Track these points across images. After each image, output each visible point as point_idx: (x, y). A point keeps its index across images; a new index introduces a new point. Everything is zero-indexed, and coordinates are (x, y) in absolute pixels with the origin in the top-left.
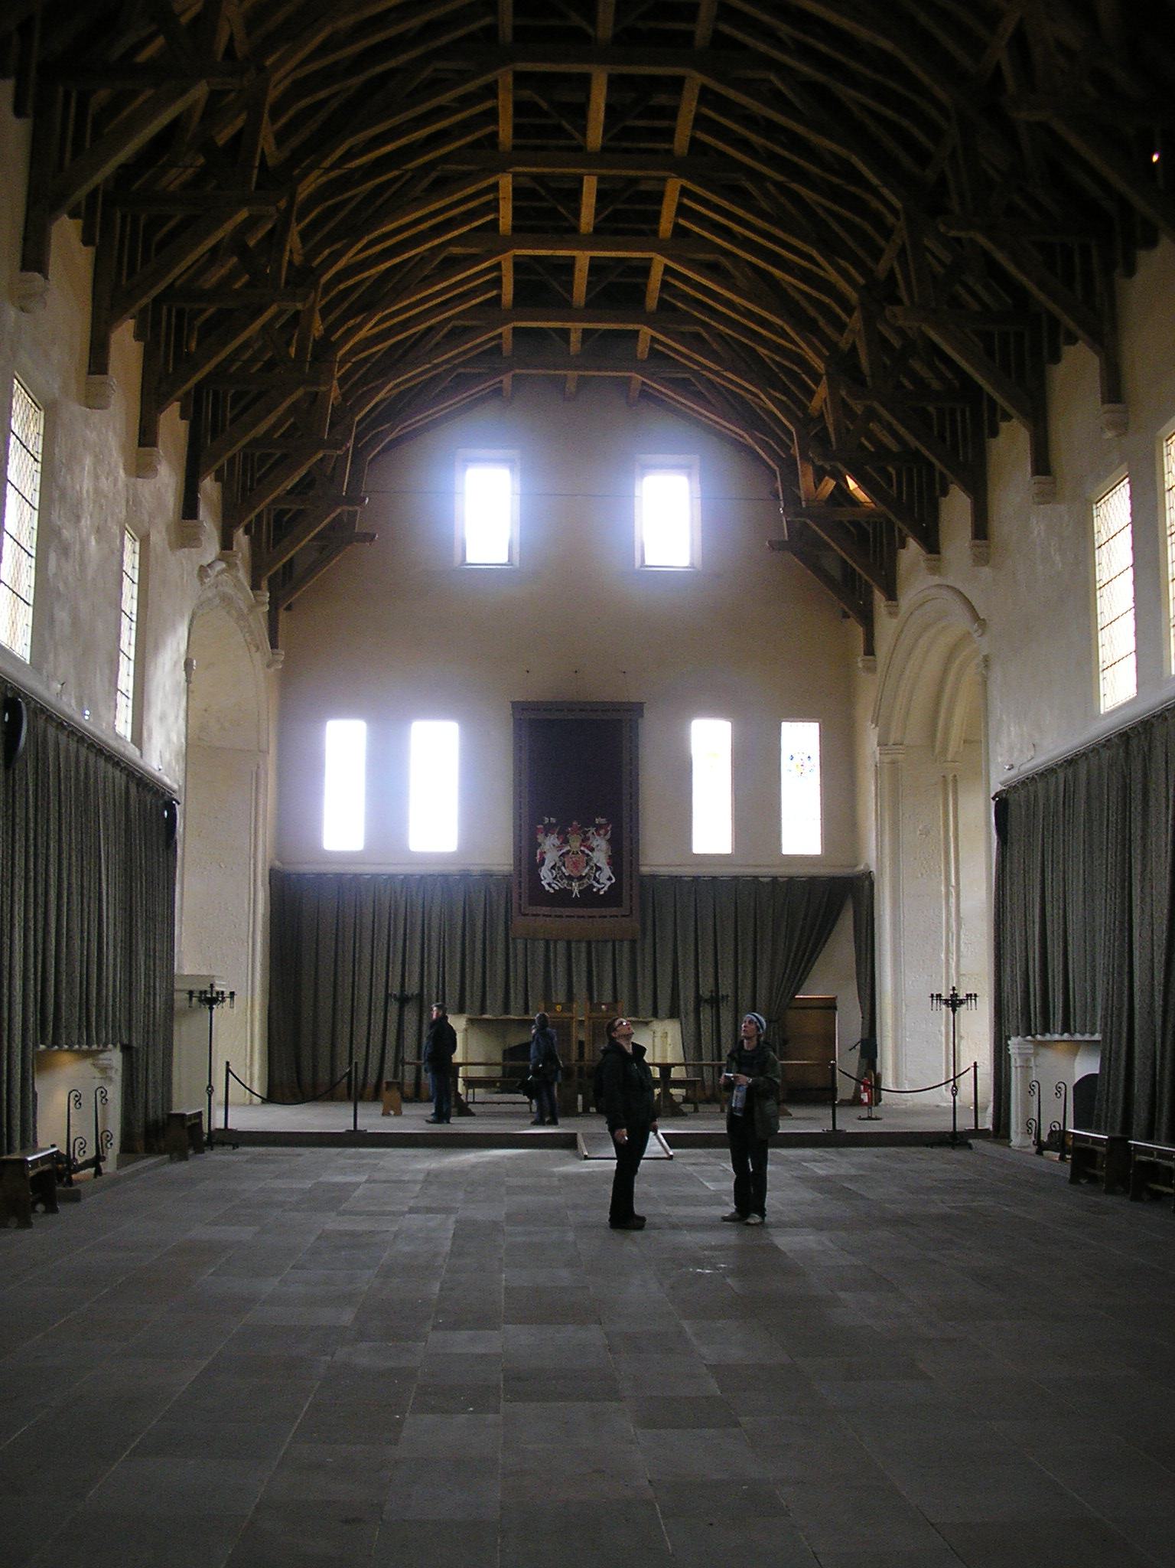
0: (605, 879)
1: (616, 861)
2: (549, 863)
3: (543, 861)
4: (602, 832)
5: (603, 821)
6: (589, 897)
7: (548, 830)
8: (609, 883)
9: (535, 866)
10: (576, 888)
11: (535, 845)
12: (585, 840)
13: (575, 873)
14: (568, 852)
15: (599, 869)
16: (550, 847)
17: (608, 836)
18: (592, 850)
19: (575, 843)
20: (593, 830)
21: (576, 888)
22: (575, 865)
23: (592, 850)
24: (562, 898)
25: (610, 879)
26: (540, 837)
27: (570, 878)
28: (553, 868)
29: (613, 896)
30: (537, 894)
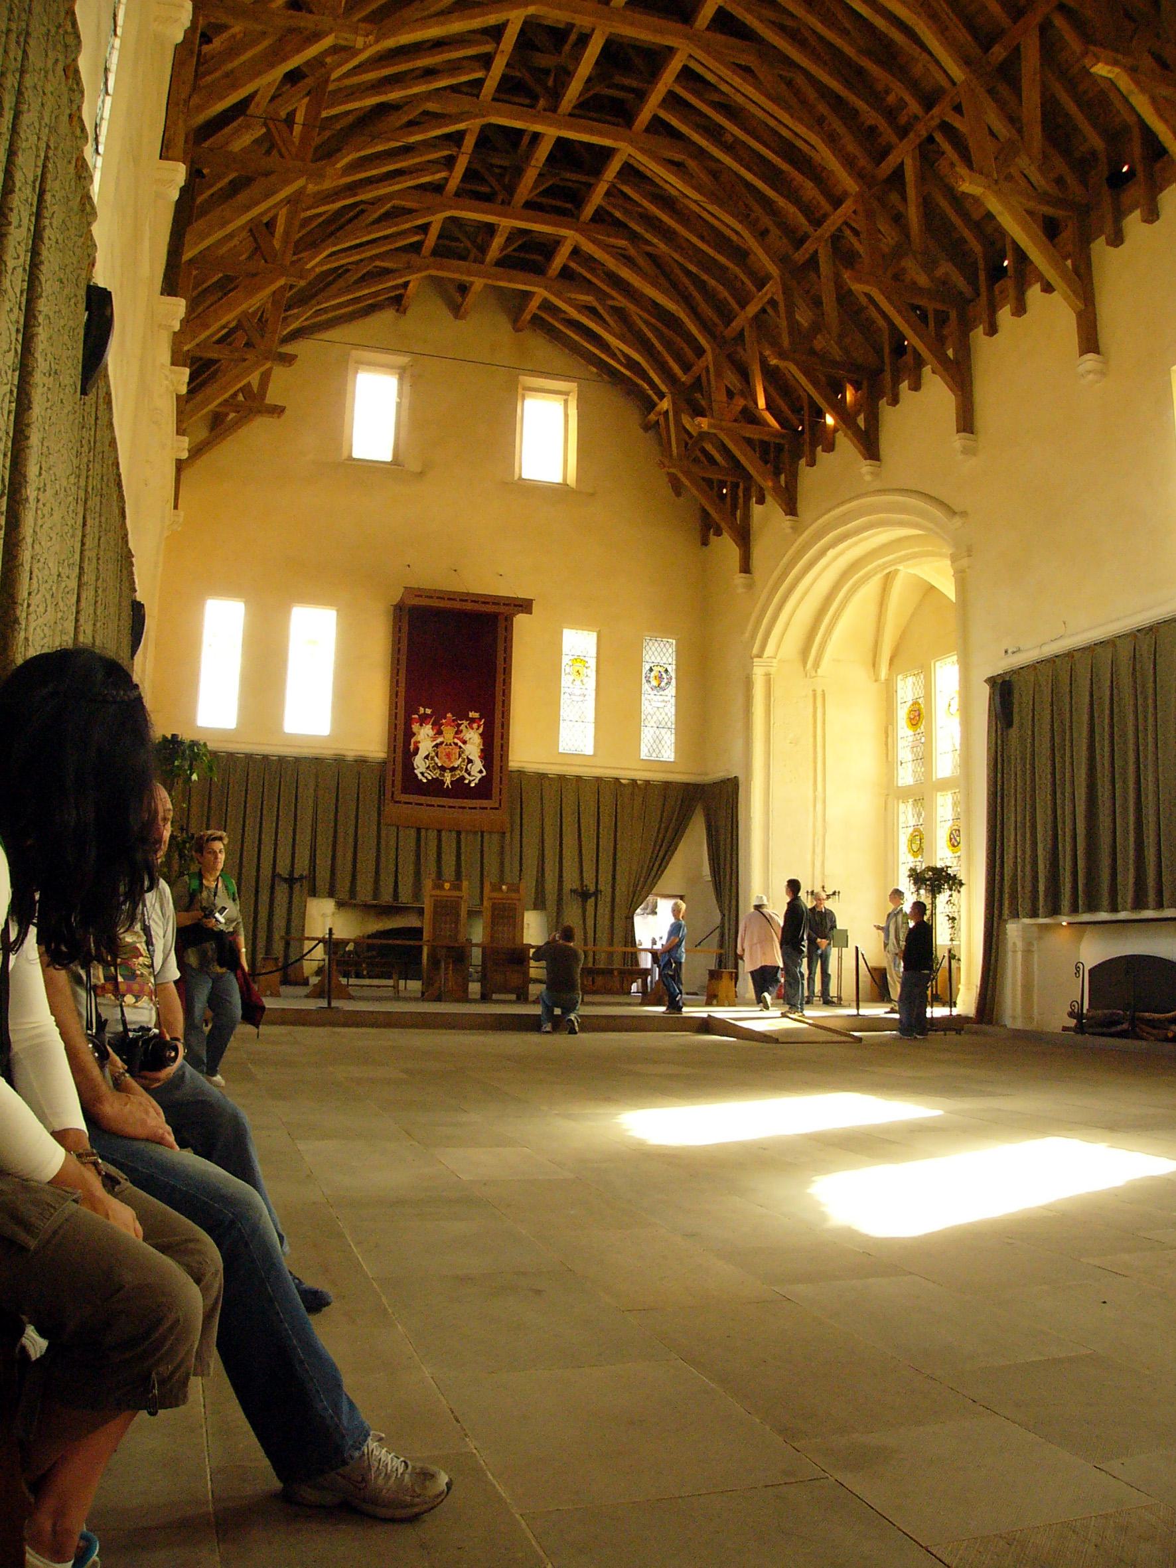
0: (476, 773)
1: (487, 755)
2: (422, 753)
3: (417, 750)
4: (475, 726)
5: (477, 715)
6: (460, 789)
7: (423, 720)
8: (479, 776)
9: (409, 754)
10: (448, 779)
11: (409, 734)
12: (458, 732)
13: (448, 764)
14: (442, 743)
15: (470, 761)
16: (425, 737)
17: (481, 730)
18: (465, 742)
19: (449, 734)
20: (466, 723)
21: (448, 779)
23: (465, 742)
24: (435, 787)
25: (481, 772)
26: (415, 727)
27: (443, 769)
28: (427, 757)
29: (484, 789)
30: (411, 783)
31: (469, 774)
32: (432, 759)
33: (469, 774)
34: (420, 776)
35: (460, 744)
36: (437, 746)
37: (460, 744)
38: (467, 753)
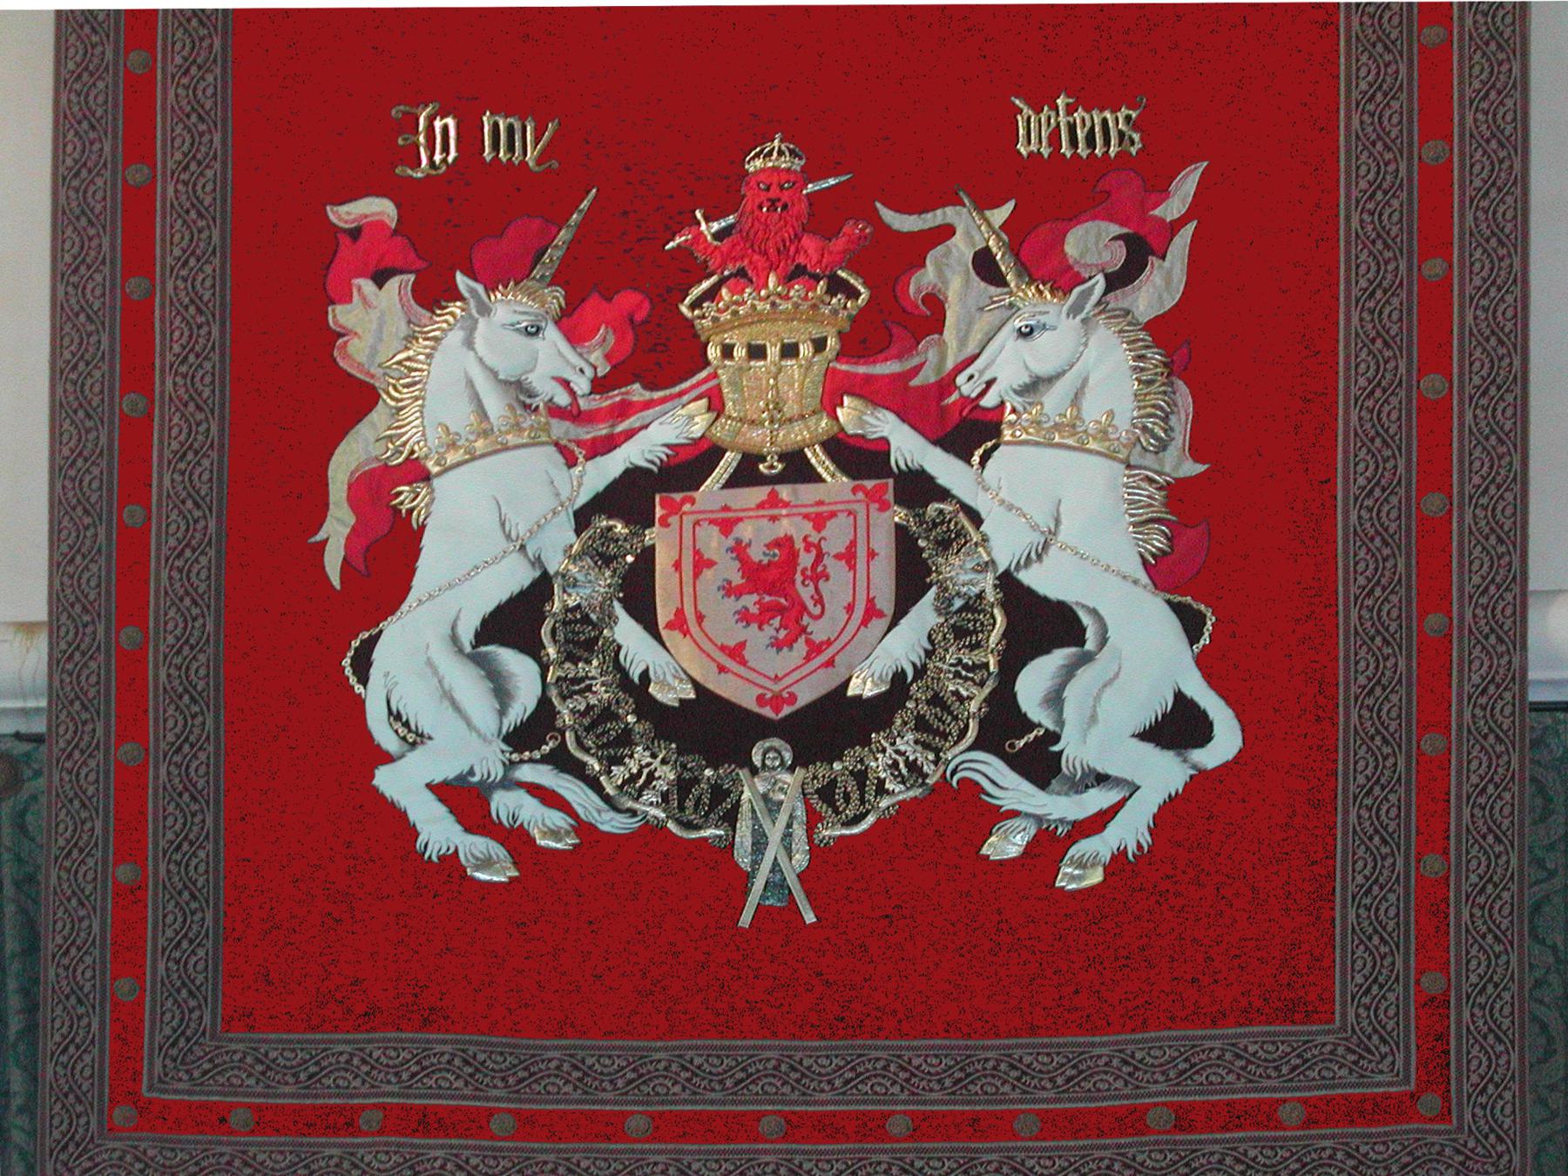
3: (390, 555)
4: (1092, 243)
10: (774, 826)
12: (893, 321)
13: (769, 675)
15: (1043, 625)
17: (1161, 286)
18: (972, 432)
20: (974, 228)
21: (774, 826)
22: (775, 586)
23: (972, 432)
27: (711, 731)
28: (514, 623)
31: (1041, 764)
32: (584, 637)
33: (1041, 764)
34: (438, 831)
35: (908, 447)
36: (632, 497)
37: (908, 447)
38: (1005, 542)
